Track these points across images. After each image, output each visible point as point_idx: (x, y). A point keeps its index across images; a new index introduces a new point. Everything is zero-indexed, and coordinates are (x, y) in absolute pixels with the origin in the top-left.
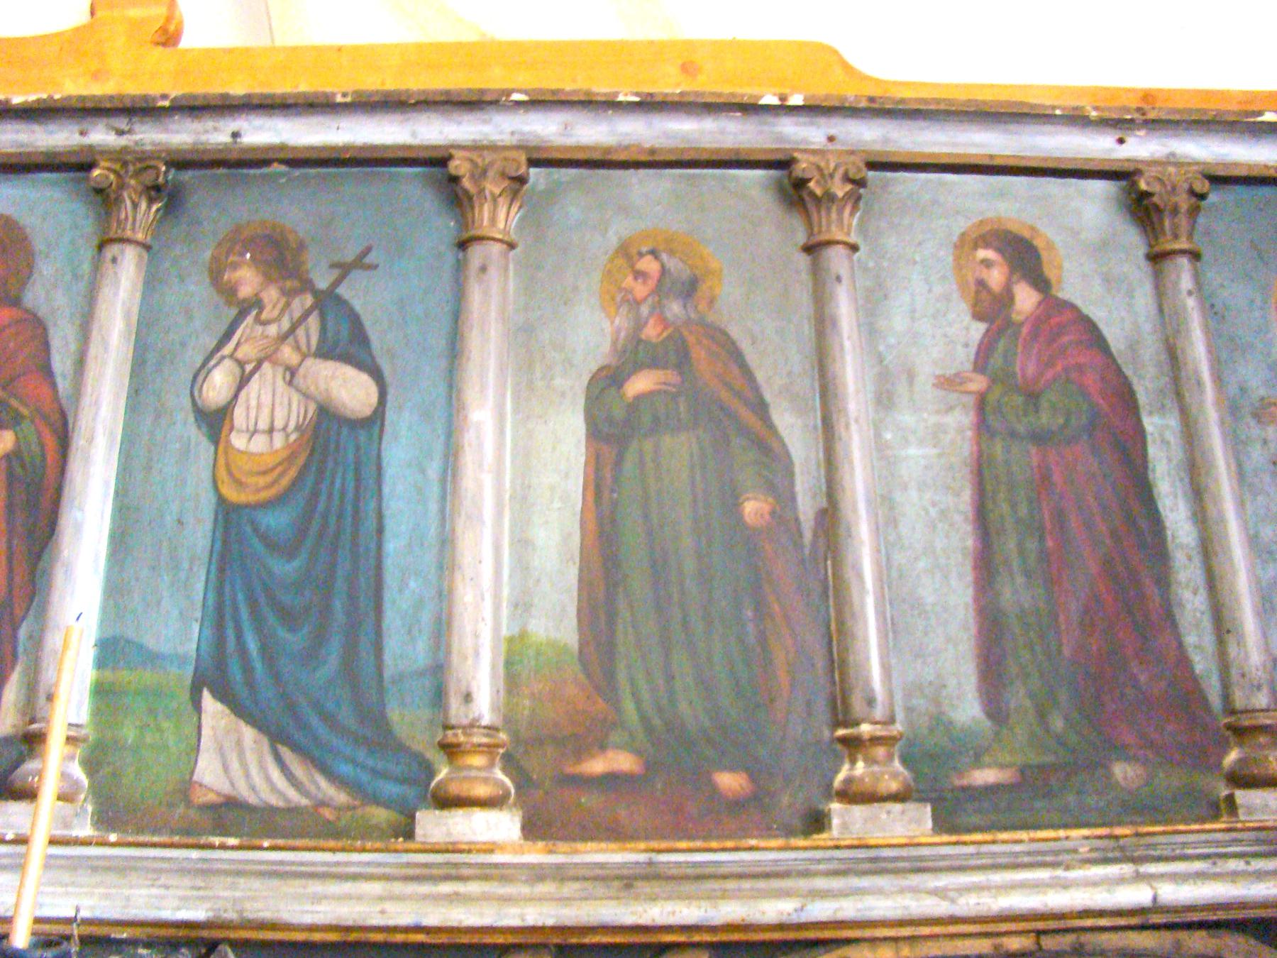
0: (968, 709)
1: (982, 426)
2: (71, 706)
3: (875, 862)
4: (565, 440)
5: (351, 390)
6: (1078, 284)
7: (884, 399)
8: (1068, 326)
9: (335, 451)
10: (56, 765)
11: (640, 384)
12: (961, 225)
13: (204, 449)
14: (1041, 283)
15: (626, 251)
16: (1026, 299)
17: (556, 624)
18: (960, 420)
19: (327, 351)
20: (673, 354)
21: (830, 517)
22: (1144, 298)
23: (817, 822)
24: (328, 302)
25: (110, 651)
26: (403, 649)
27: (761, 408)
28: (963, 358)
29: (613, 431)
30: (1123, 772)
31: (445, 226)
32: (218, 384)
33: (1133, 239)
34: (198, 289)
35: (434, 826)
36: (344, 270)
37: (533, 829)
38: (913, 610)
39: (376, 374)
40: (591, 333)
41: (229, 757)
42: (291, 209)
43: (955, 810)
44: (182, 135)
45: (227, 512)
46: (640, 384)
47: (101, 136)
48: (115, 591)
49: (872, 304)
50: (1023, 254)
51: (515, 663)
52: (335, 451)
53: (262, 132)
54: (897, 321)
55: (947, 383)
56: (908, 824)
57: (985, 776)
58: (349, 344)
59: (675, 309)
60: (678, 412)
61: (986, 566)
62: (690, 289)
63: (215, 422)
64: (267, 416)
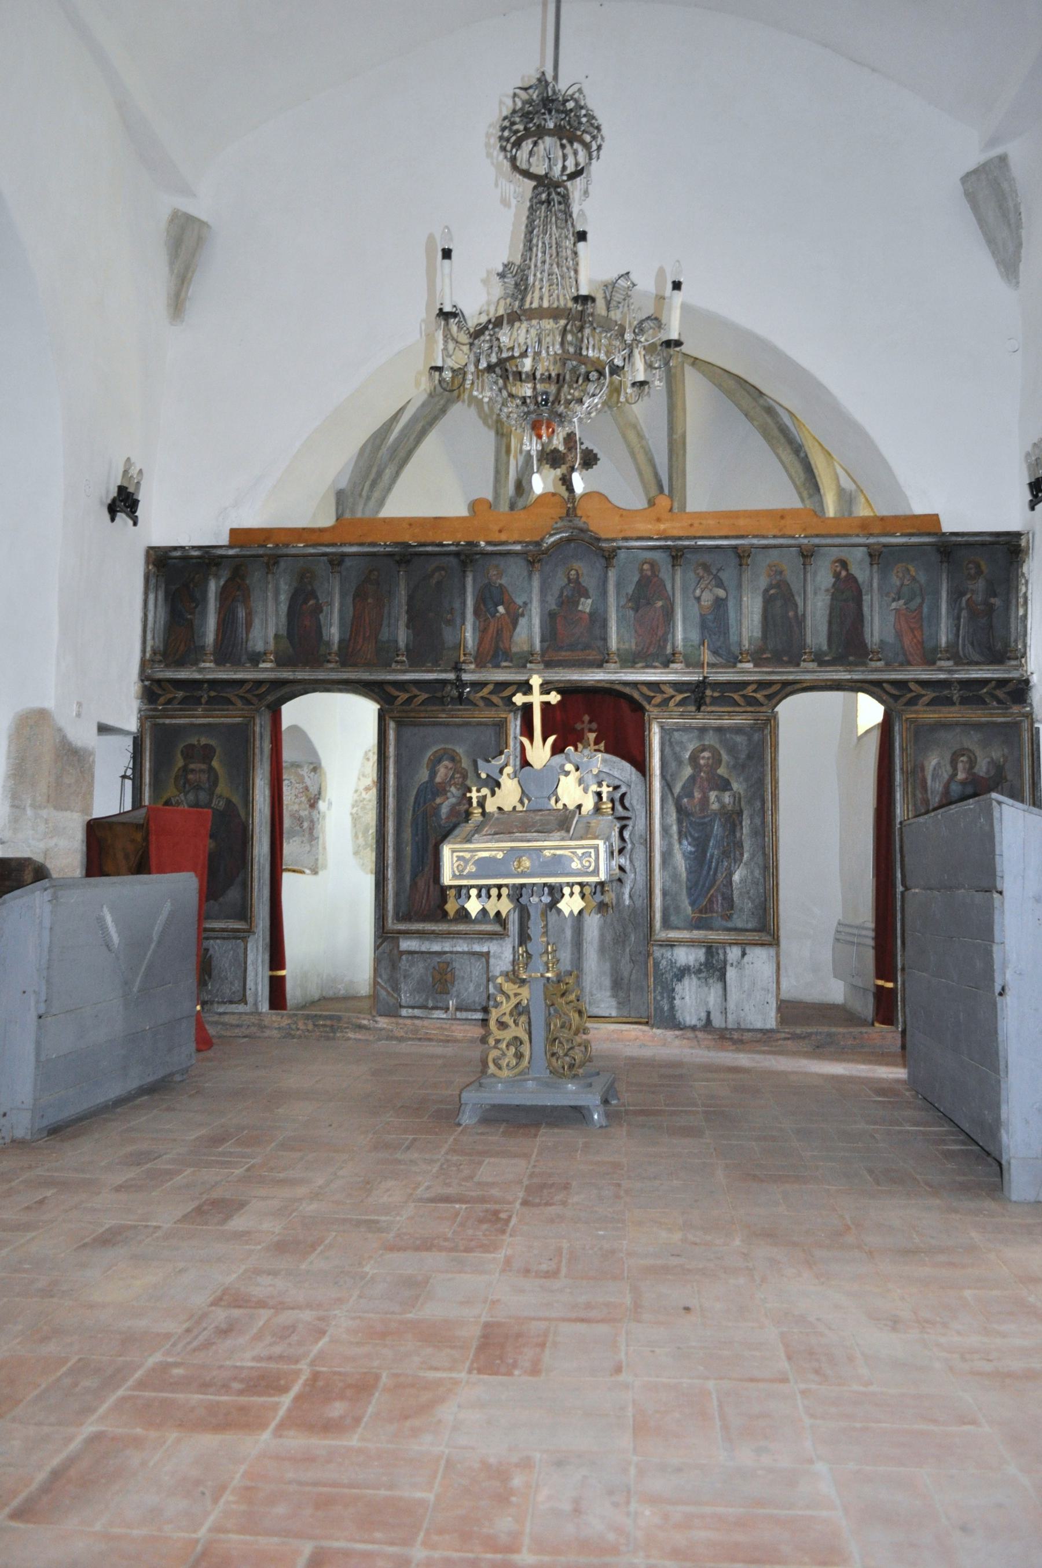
0: (825, 648)
1: (832, 599)
5: (721, 593)
6: (854, 570)
7: (815, 593)
8: (852, 579)
9: (720, 604)
11: (772, 592)
12: (833, 558)
13: (696, 605)
14: (847, 570)
15: (769, 566)
17: (757, 633)
18: (829, 597)
19: (718, 586)
20: (778, 586)
21: (804, 615)
22: (867, 572)
23: (798, 665)
24: (716, 577)
27: (793, 596)
28: (830, 585)
30: (851, 658)
32: (698, 592)
33: (867, 559)
34: (692, 575)
35: (739, 665)
36: (719, 570)
37: (755, 666)
39: (725, 589)
40: (763, 582)
41: (707, 656)
42: (707, 558)
45: (701, 615)
46: (772, 592)
47: (669, 543)
48: (685, 630)
49: (815, 574)
50: (844, 564)
51: (750, 639)
52: (720, 604)
53: (700, 543)
54: (818, 578)
55: (827, 590)
56: (812, 666)
57: (827, 658)
58: (720, 584)
59: (778, 577)
61: (830, 623)
62: (781, 573)
63: (698, 599)
64: (707, 599)
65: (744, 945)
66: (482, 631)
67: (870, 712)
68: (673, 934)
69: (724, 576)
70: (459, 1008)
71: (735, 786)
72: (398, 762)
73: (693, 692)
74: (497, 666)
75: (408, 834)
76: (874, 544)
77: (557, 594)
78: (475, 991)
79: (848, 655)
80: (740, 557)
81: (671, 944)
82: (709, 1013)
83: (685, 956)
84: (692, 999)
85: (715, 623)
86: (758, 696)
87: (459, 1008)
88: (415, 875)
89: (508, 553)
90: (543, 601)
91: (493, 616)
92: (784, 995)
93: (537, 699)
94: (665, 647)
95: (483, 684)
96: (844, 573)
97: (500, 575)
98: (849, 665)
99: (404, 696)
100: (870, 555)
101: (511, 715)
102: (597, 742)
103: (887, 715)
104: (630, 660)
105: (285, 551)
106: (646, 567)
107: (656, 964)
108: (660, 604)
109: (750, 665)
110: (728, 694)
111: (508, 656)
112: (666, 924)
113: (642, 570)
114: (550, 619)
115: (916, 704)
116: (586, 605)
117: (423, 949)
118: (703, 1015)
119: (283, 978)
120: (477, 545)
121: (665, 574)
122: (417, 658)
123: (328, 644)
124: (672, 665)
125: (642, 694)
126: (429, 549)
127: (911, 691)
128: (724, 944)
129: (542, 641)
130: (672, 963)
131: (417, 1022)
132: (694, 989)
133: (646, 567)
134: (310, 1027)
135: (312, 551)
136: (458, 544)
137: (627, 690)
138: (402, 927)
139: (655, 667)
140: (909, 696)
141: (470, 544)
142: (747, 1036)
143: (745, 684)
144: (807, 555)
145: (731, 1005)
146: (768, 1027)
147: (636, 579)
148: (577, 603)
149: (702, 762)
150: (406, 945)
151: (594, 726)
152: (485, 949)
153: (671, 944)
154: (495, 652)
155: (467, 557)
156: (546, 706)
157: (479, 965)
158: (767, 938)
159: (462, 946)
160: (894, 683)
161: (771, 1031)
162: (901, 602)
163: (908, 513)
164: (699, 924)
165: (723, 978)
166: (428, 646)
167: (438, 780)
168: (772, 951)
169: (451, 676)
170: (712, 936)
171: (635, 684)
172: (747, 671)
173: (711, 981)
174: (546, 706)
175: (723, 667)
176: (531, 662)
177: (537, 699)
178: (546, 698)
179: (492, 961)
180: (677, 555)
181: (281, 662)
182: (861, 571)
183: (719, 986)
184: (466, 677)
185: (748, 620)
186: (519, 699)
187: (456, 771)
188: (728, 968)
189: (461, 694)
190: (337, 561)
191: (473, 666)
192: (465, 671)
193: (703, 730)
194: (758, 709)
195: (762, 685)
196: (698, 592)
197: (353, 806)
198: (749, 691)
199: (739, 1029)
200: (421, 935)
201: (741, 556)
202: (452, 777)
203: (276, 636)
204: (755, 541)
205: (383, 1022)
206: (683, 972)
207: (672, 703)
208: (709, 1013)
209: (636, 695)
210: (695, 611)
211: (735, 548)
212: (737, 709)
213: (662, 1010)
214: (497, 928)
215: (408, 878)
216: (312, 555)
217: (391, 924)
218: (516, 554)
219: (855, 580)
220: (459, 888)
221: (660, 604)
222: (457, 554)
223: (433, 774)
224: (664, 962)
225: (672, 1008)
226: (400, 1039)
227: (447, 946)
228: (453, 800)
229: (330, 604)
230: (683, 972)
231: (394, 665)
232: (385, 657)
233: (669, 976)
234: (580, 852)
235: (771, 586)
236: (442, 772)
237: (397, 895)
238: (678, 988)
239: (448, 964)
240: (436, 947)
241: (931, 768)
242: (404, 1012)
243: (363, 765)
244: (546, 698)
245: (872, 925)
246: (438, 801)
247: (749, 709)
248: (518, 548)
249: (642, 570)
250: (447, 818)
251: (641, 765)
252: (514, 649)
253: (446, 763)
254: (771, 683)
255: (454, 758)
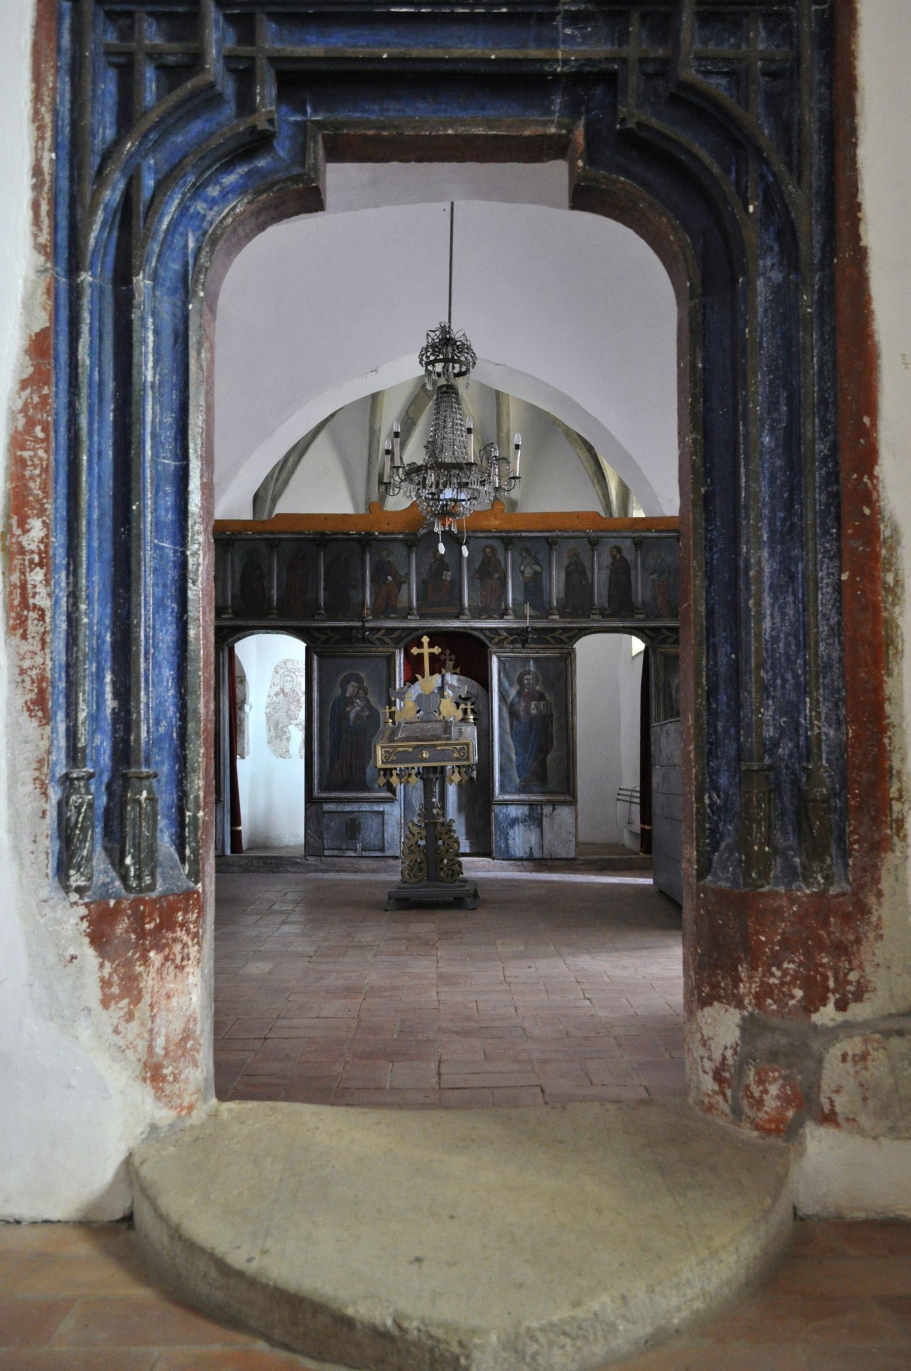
0: (606, 605)
2: (510, 605)
3: (594, 621)
4: (563, 575)
5: (538, 569)
7: (599, 569)
9: (537, 576)
10: (510, 612)
11: (571, 568)
14: (621, 554)
15: (570, 550)
16: (618, 556)
17: (562, 595)
18: (608, 572)
21: (592, 585)
24: (534, 557)
25: (513, 599)
26: (546, 598)
27: (585, 571)
29: (568, 574)
31: (547, 547)
32: (522, 567)
33: (634, 547)
35: (550, 617)
36: (536, 553)
38: (600, 593)
40: (566, 561)
41: (528, 610)
43: (604, 615)
44: (514, 534)
46: (571, 568)
47: (503, 534)
50: (618, 549)
53: (524, 534)
55: (608, 567)
58: (537, 563)
60: (577, 576)
62: (577, 555)
63: (523, 572)
64: (528, 572)
65: (554, 804)
66: (375, 593)
67: (638, 645)
68: (507, 797)
69: (539, 557)
70: (363, 850)
71: (548, 698)
72: (319, 683)
73: (519, 635)
74: (387, 617)
75: (327, 732)
76: (638, 537)
77: (428, 567)
78: (375, 837)
79: (621, 613)
80: (550, 545)
81: (506, 803)
82: (531, 848)
83: (514, 811)
84: (520, 840)
85: (534, 591)
86: (563, 637)
87: (363, 850)
88: (332, 761)
89: (395, 540)
90: (417, 574)
91: (385, 583)
92: (581, 838)
93: (426, 651)
94: (500, 605)
95: (378, 629)
96: (618, 556)
97: (389, 555)
98: (623, 618)
99: (324, 637)
100: (635, 544)
101: (397, 651)
102: (455, 667)
103: (646, 648)
104: (477, 613)
105: (239, 537)
106: (488, 550)
107: (497, 817)
108: (497, 575)
109: (557, 617)
110: (543, 636)
111: (394, 610)
112: (503, 790)
113: (484, 553)
114: (423, 585)
115: (666, 643)
116: (447, 576)
117: (339, 810)
118: (528, 850)
119: (240, 832)
120: (374, 534)
121: (500, 556)
122: (333, 611)
123: (270, 601)
124: (506, 617)
125: (486, 636)
126: (339, 536)
127: (663, 634)
128: (541, 804)
129: (417, 600)
130: (507, 816)
131: (334, 859)
132: (521, 833)
133: (488, 550)
134: (261, 864)
135: (258, 537)
136: (360, 534)
137: (476, 633)
138: (324, 795)
139: (495, 618)
140: (661, 637)
141: (369, 534)
142: (556, 863)
143: (554, 629)
144: (594, 543)
145: (546, 843)
146: (570, 856)
147: (481, 558)
148: (442, 575)
149: (526, 682)
150: (327, 807)
151: (453, 657)
152: (381, 809)
153: (506, 803)
154: (385, 608)
155: (365, 541)
156: (432, 655)
157: (377, 819)
158: (569, 798)
159: (366, 807)
160: (651, 629)
161: (573, 859)
162: (656, 575)
163: (662, 515)
164: (523, 789)
165: (540, 825)
166: (340, 603)
167: (348, 695)
168: (573, 808)
169: (359, 624)
170: (533, 797)
171: (481, 630)
172: (556, 621)
173: (532, 827)
174: (432, 655)
175: (541, 618)
176: (411, 615)
177: (426, 651)
178: (432, 650)
179: (386, 817)
180: (508, 541)
181: (237, 615)
182: (629, 554)
183: (538, 830)
184: (367, 625)
185: (556, 585)
186: (415, 651)
187: (360, 688)
188: (544, 818)
189: (364, 637)
190: (273, 544)
191: (371, 617)
192: (368, 621)
193: (527, 659)
194: (561, 646)
195: (565, 630)
196: (522, 567)
197: (267, 708)
198: (557, 634)
199: (551, 859)
200: (338, 801)
201: (551, 543)
202: (358, 693)
203: (233, 596)
204: (560, 534)
205: (311, 860)
206: (513, 822)
207: (505, 642)
208: (531, 848)
209: (482, 637)
210: (520, 580)
211: (546, 538)
212: (549, 646)
213: (500, 847)
214: (389, 795)
215: (328, 762)
216: (258, 539)
217: (316, 792)
218: (400, 540)
219: (626, 559)
220: (385, 770)
221: (497, 575)
222: (359, 541)
223: (344, 691)
224: (501, 815)
225: (507, 845)
226: (324, 871)
227: (355, 807)
228: (358, 708)
229: (270, 573)
230: (513, 822)
231: (316, 617)
232: (312, 610)
233: (505, 825)
234: (458, 747)
235: (570, 564)
236: (350, 690)
237: (321, 772)
238: (511, 832)
239: (355, 819)
240: (348, 808)
241: (675, 685)
242: (326, 853)
243: (273, 677)
244: (432, 650)
245: (638, 789)
246: (348, 709)
247: (556, 646)
248: (401, 536)
249: (484, 553)
250: (355, 721)
251: (486, 684)
252: (399, 605)
253: (353, 683)
254: (572, 629)
255: (359, 680)
